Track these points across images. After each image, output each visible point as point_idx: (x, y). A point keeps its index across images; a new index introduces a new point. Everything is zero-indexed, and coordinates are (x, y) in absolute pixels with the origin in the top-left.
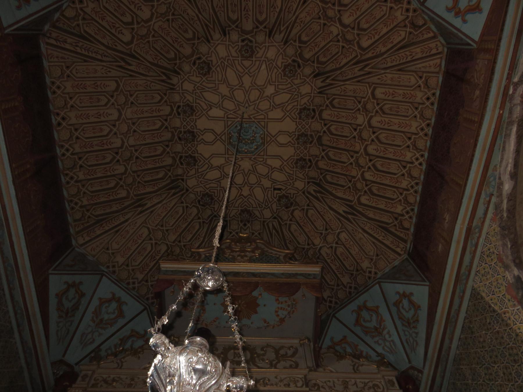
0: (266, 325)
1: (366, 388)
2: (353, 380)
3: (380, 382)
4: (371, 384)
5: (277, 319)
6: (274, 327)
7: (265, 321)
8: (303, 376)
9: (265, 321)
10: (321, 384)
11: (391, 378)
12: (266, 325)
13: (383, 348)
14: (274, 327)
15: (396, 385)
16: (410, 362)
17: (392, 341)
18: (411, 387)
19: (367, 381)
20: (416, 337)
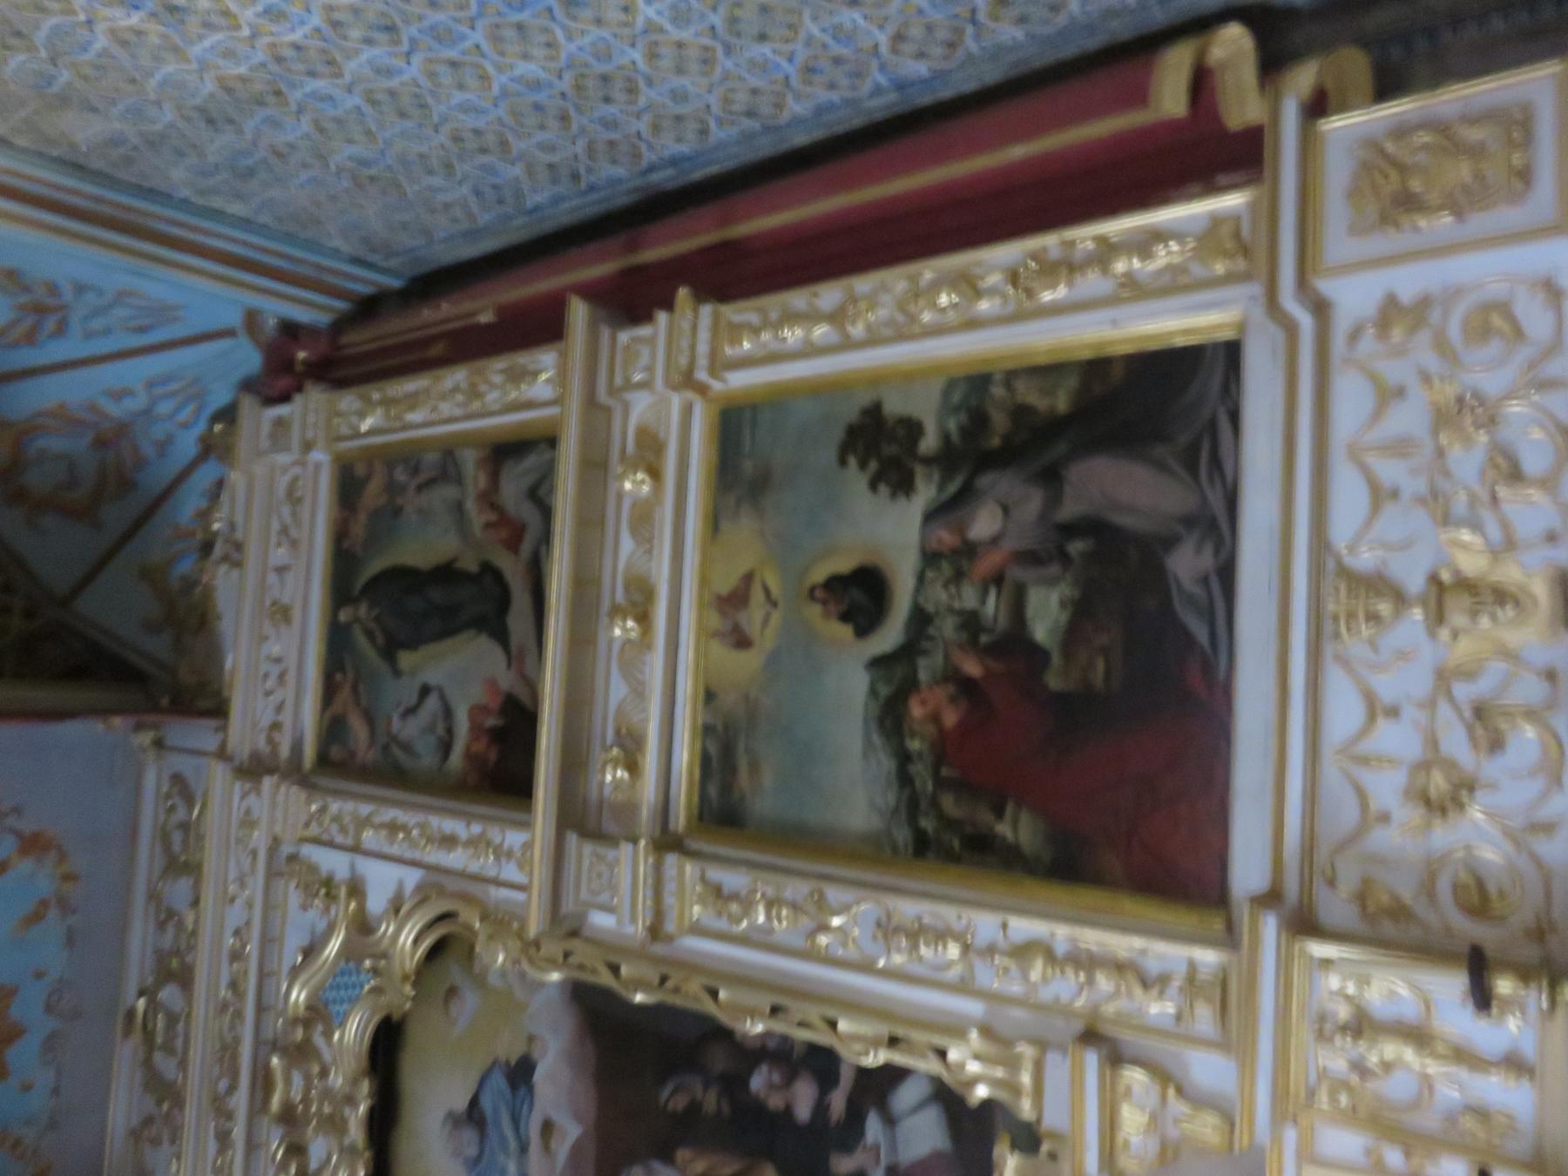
0: (53, 914)
1: (293, 532)
2: (272, 578)
3: (285, 470)
4: (286, 511)
5: (24, 866)
6: (68, 877)
7: (36, 917)
8: (238, 786)
9: (36, 917)
10: (267, 719)
11: (266, 428)
12: (53, 914)
13: (185, 426)
14: (68, 877)
15: (282, 410)
16: (228, 333)
17: (150, 385)
18: (302, 355)
19: (275, 526)
20: (100, 292)
